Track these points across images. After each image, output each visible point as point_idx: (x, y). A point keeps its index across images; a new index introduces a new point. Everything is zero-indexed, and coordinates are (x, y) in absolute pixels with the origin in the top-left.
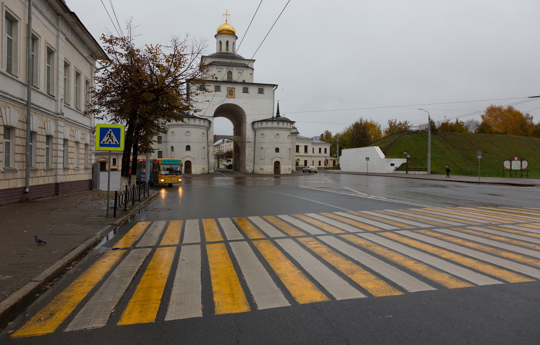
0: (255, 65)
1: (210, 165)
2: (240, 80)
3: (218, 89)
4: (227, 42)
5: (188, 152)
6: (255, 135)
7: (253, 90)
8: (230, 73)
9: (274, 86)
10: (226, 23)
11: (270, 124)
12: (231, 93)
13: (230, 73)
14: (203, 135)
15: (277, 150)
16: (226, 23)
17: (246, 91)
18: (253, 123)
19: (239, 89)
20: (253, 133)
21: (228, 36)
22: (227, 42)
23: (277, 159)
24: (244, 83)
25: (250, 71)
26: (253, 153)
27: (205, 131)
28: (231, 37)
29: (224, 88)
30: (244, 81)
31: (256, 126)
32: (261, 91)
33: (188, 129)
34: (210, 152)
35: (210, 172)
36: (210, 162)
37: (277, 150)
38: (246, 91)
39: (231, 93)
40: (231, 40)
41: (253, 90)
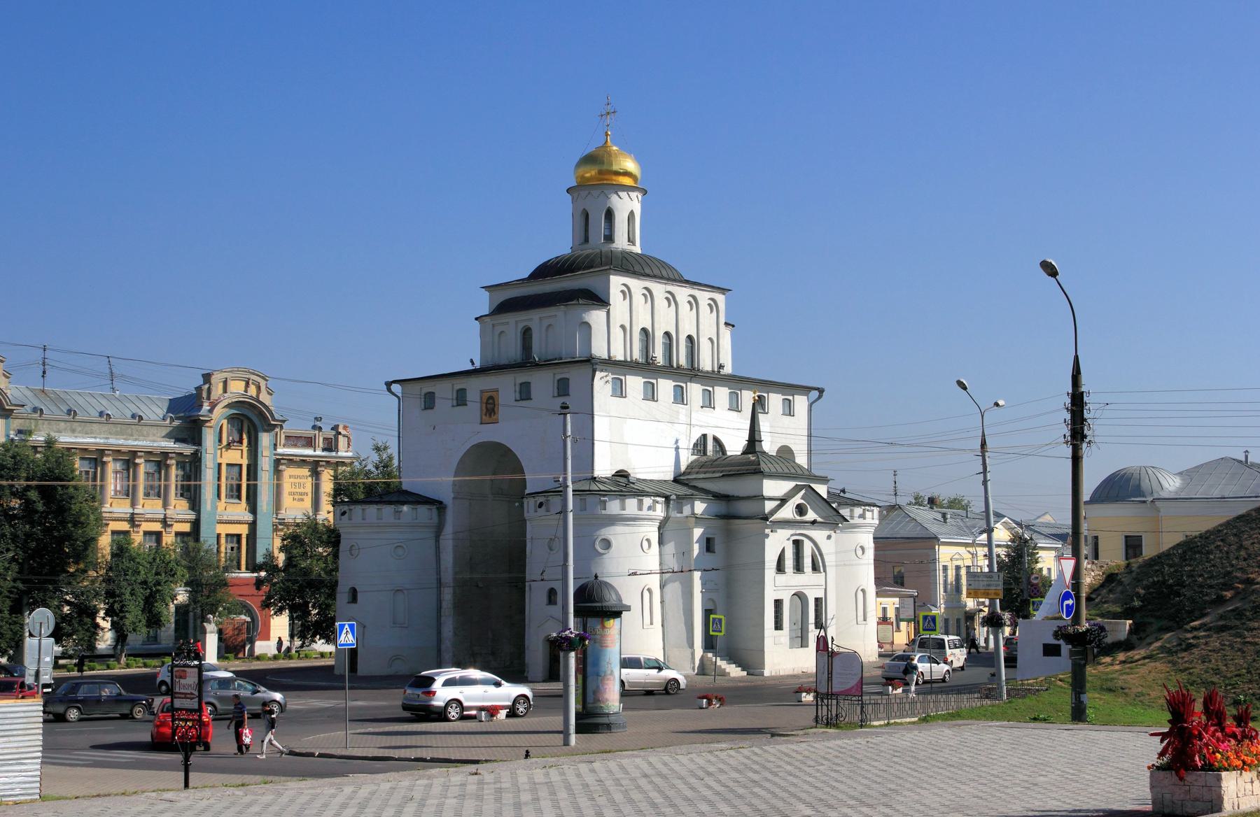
8: (527, 333)
12: (490, 408)
13: (527, 333)
14: (400, 551)
34: (444, 604)
39: (490, 408)
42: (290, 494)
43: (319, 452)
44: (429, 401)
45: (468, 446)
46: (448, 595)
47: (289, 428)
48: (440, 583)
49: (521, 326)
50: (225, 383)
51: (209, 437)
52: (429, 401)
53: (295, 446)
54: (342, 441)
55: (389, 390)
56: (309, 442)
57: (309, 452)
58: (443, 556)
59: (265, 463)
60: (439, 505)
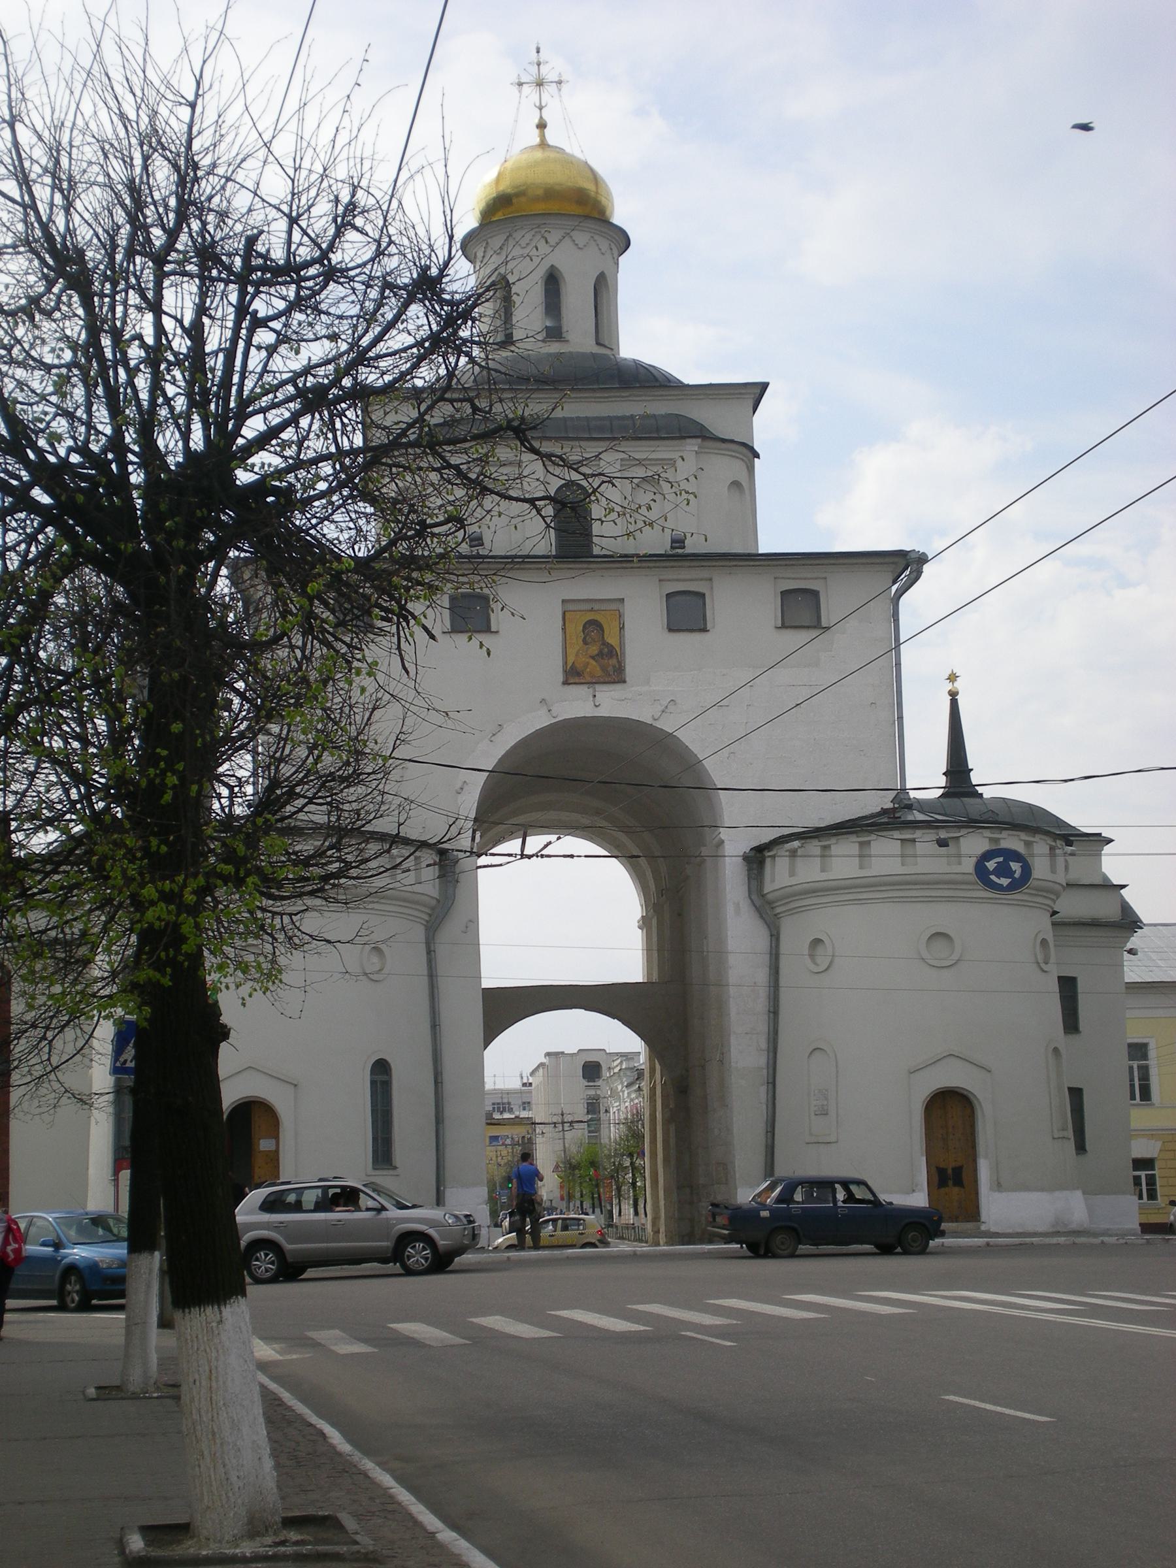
0: (767, 426)
2: (654, 541)
4: (553, 281)
9: (904, 566)
10: (543, 144)
16: (543, 144)
17: (687, 614)
18: (757, 858)
22: (553, 281)
24: (678, 555)
25: (724, 467)
28: (581, 237)
30: (678, 542)
31: (780, 874)
38: (687, 614)
40: (575, 261)
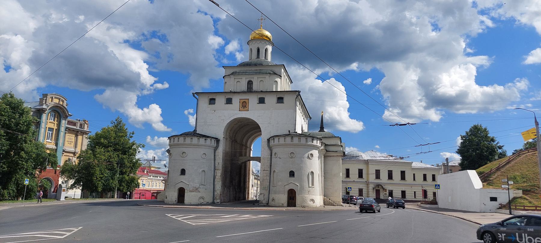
1: (216, 193)
3: (229, 101)
4: (258, 50)
5: (182, 176)
6: (271, 155)
7: (271, 100)
8: (250, 83)
11: (282, 140)
12: (244, 105)
13: (250, 83)
15: (292, 174)
17: (262, 101)
19: (253, 100)
20: (269, 152)
21: (258, 42)
22: (258, 50)
23: (291, 187)
26: (268, 178)
27: (210, 152)
29: (236, 100)
32: (280, 100)
33: (184, 150)
34: (217, 177)
35: (215, 201)
36: (216, 189)
37: (292, 174)
38: (262, 101)
39: (244, 105)
41: (271, 100)
42: (68, 141)
43: (78, 128)
44: (212, 101)
45: (232, 118)
46: (219, 173)
47: (69, 119)
48: (215, 169)
49: (248, 80)
50: (52, 98)
51: (44, 116)
52: (212, 101)
53: (69, 125)
54: (86, 126)
55: (194, 96)
56: (75, 124)
57: (75, 127)
58: (217, 158)
59: (63, 129)
60: (218, 140)
